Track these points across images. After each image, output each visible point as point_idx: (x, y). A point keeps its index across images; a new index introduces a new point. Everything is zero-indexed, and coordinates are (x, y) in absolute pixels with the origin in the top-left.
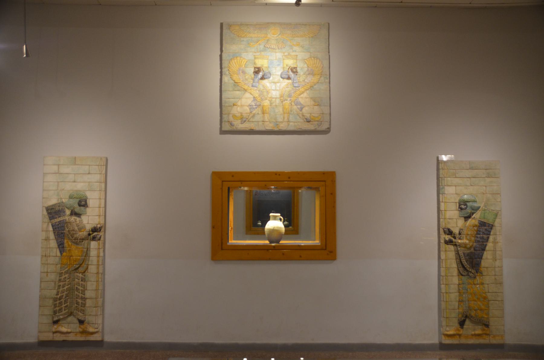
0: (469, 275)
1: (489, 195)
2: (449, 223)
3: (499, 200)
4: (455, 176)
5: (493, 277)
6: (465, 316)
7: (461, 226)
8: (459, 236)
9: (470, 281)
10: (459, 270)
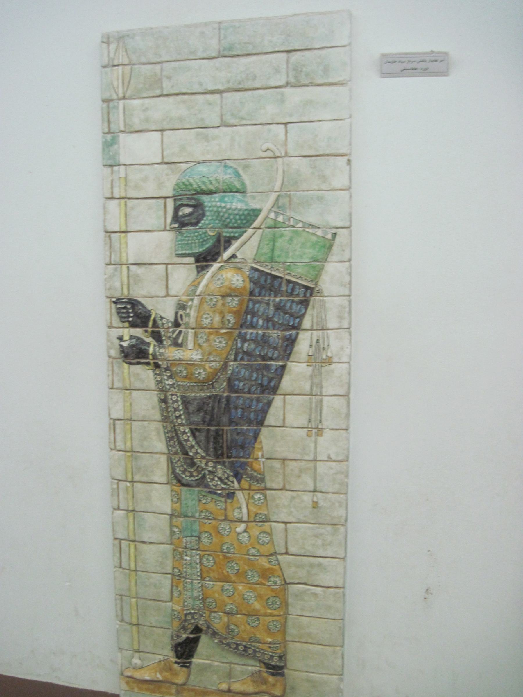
0: (207, 486)
1: (297, 163)
2: (138, 280)
3: (341, 181)
4: (158, 92)
5: (307, 498)
6: (191, 628)
7: (183, 295)
8: (173, 332)
9: (211, 506)
10: (170, 461)
